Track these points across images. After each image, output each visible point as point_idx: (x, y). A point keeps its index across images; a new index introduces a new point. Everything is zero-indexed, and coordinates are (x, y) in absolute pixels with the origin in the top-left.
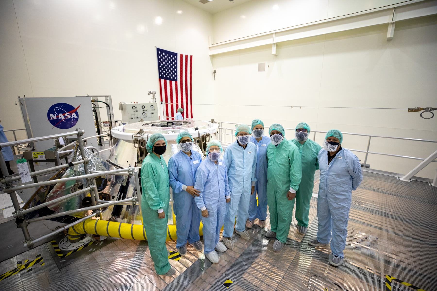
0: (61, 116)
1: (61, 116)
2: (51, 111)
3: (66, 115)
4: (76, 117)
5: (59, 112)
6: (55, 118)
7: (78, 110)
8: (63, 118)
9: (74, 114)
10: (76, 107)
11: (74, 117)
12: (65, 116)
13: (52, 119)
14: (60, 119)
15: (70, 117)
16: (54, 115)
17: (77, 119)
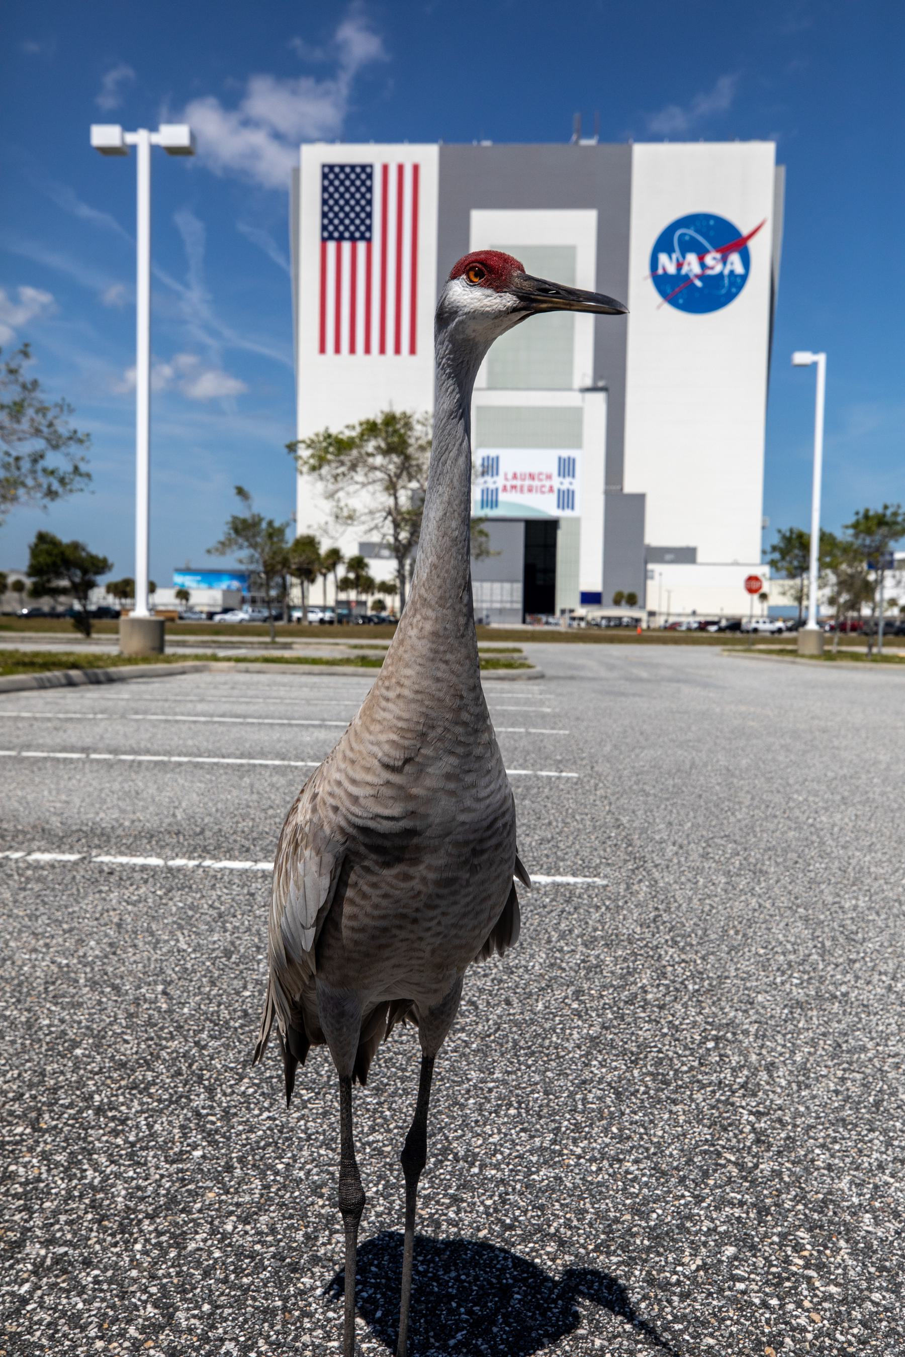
0: (692, 265)
1: (692, 265)
2: (664, 244)
3: (709, 260)
4: (739, 269)
5: (688, 246)
6: (672, 269)
7: (752, 244)
8: (696, 269)
9: (735, 260)
10: (745, 232)
11: (732, 272)
12: (703, 266)
13: (660, 271)
14: (687, 276)
15: (718, 269)
16: (670, 258)
17: (744, 278)
